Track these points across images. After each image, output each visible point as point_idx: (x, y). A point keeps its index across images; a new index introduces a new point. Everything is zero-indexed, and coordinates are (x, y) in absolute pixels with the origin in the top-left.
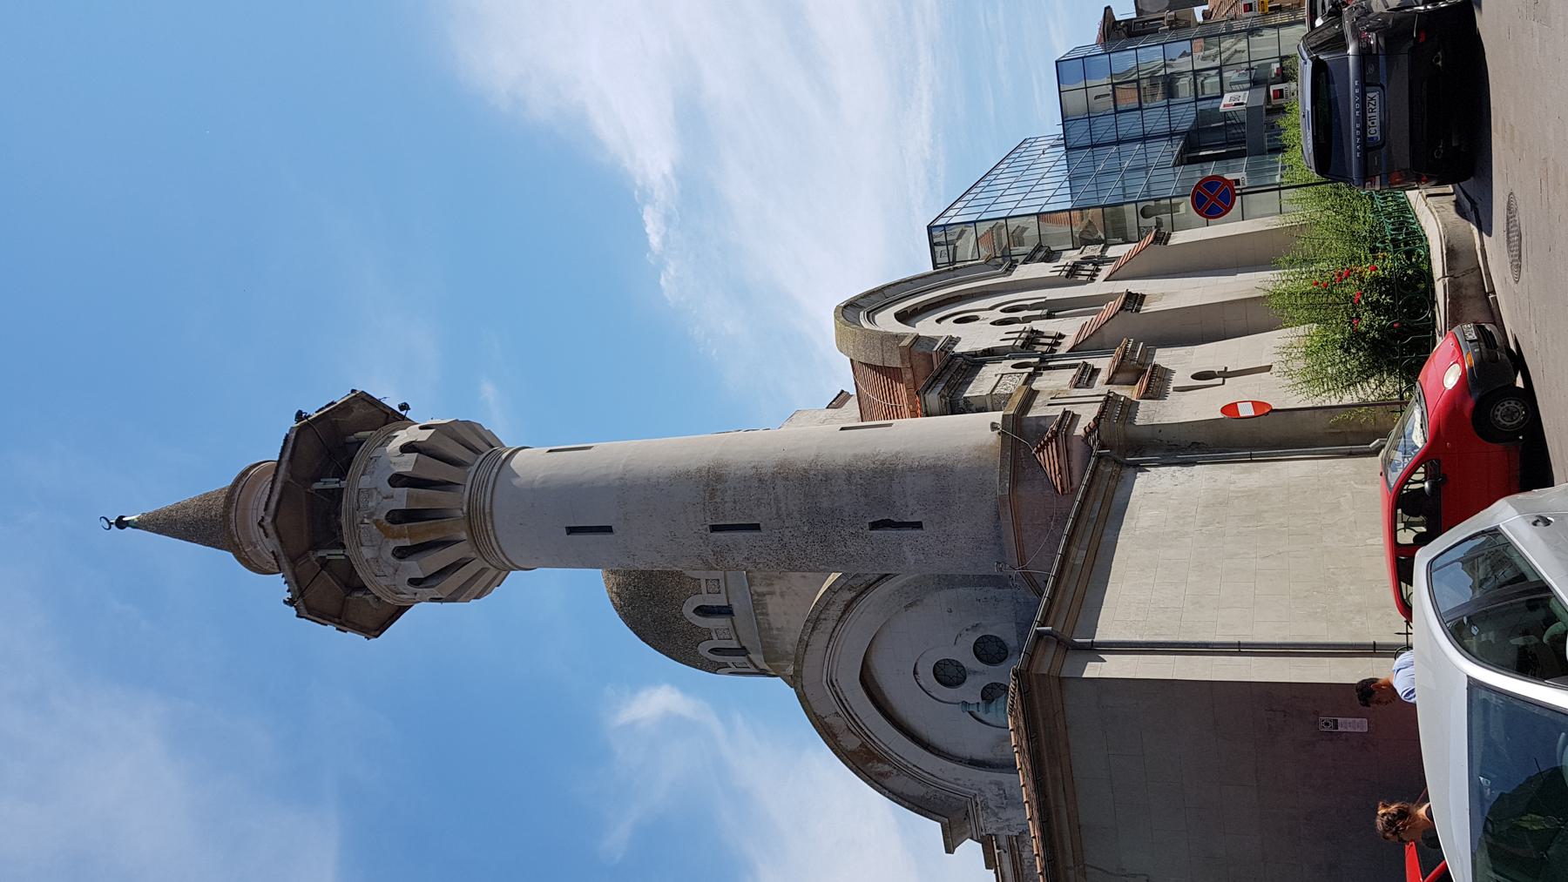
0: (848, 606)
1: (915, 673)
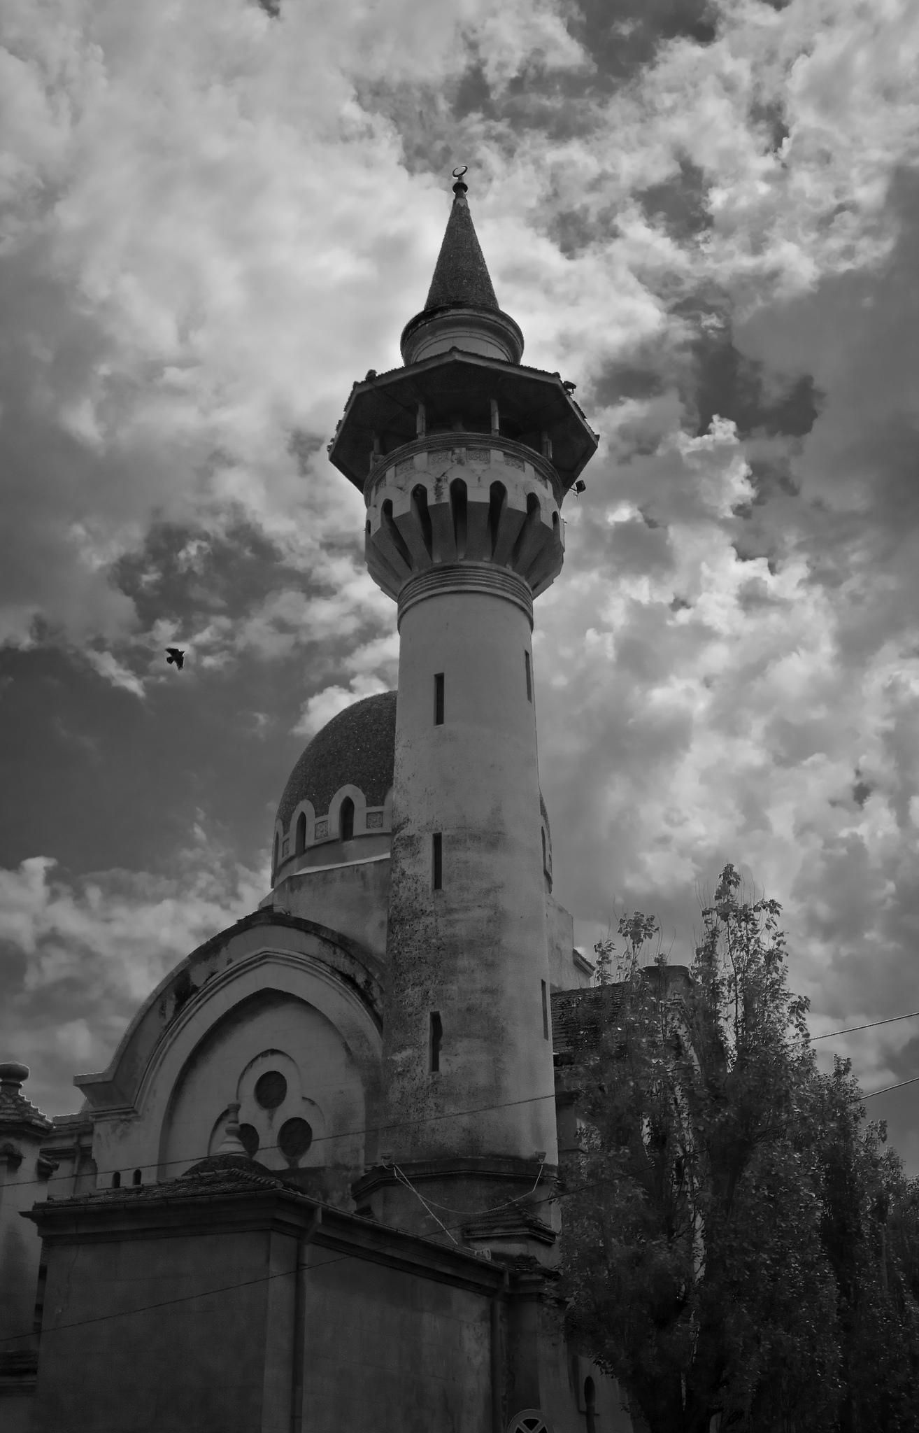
0: (349, 979)
1: (273, 1052)
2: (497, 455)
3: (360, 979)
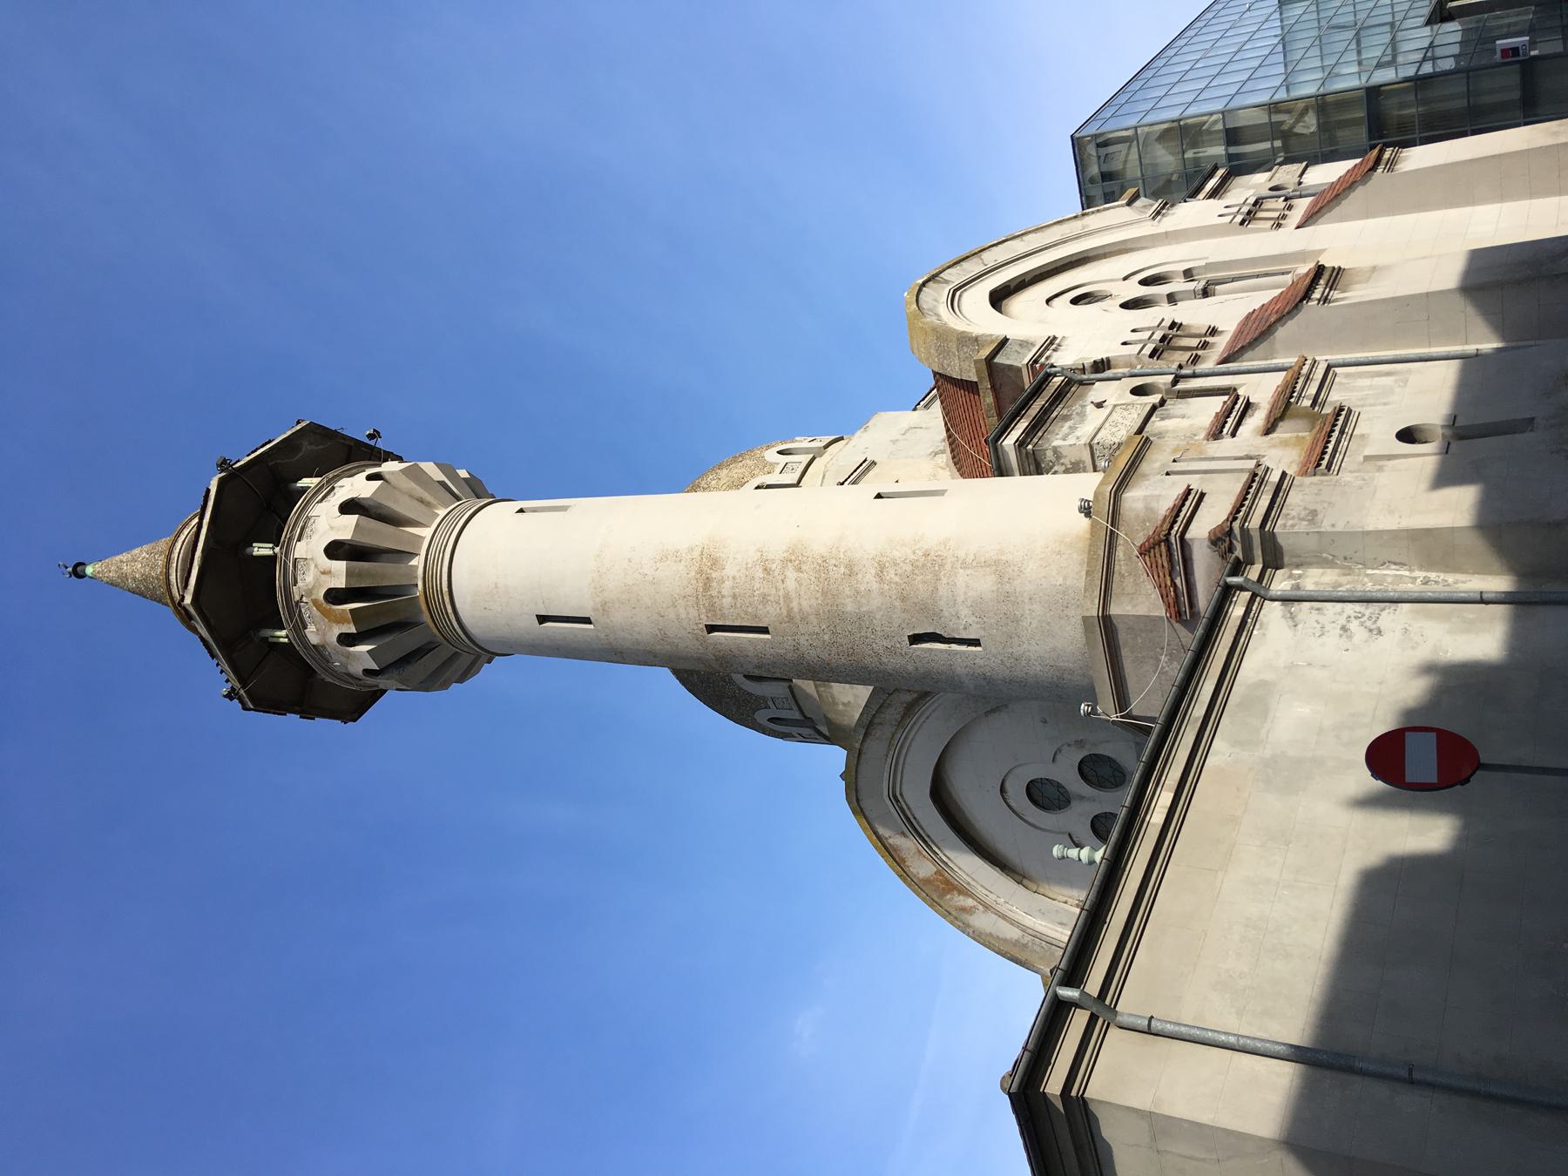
0: (910, 709)
1: (1003, 790)
2: (300, 550)
3: (908, 698)
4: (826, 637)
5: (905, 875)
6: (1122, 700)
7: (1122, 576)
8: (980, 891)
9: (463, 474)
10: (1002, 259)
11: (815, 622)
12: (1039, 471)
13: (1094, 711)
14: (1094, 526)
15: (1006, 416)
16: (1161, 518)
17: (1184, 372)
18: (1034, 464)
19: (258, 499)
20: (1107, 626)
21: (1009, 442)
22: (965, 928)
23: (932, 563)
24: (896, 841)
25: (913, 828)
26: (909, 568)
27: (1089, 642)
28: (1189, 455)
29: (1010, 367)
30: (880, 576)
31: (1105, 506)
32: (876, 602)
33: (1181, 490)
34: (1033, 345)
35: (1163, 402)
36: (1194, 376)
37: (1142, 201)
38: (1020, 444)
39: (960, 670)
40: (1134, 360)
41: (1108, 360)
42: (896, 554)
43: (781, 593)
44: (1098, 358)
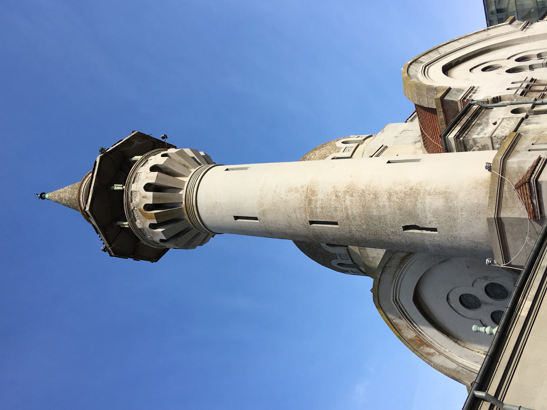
0: (403, 260)
1: (448, 299)
3: (402, 255)
4: (364, 227)
5: (401, 336)
6: (506, 257)
7: (506, 198)
8: (437, 346)
9: (202, 153)
10: (448, 51)
11: (359, 219)
12: (466, 150)
13: (493, 262)
14: (492, 175)
15: (450, 125)
16: (526, 171)
17: (538, 102)
18: (463, 147)
19: (117, 165)
20: (499, 222)
21: (451, 136)
22: (429, 362)
23: (413, 193)
24: (397, 321)
25: (405, 315)
26: (403, 195)
27: (490, 230)
28: (540, 141)
29: (452, 101)
30: (389, 199)
31: (498, 166)
32: (388, 210)
33: (536, 158)
34: (463, 91)
35: (527, 117)
36: (543, 104)
37: (517, 22)
38: (457, 137)
39: (427, 243)
40: (513, 97)
41: (500, 97)
42: (397, 189)
43: (344, 206)
44: (495, 96)
